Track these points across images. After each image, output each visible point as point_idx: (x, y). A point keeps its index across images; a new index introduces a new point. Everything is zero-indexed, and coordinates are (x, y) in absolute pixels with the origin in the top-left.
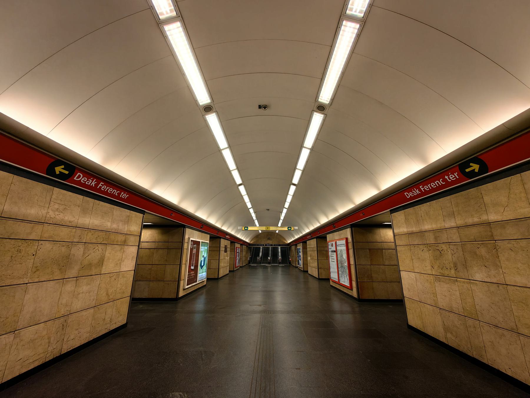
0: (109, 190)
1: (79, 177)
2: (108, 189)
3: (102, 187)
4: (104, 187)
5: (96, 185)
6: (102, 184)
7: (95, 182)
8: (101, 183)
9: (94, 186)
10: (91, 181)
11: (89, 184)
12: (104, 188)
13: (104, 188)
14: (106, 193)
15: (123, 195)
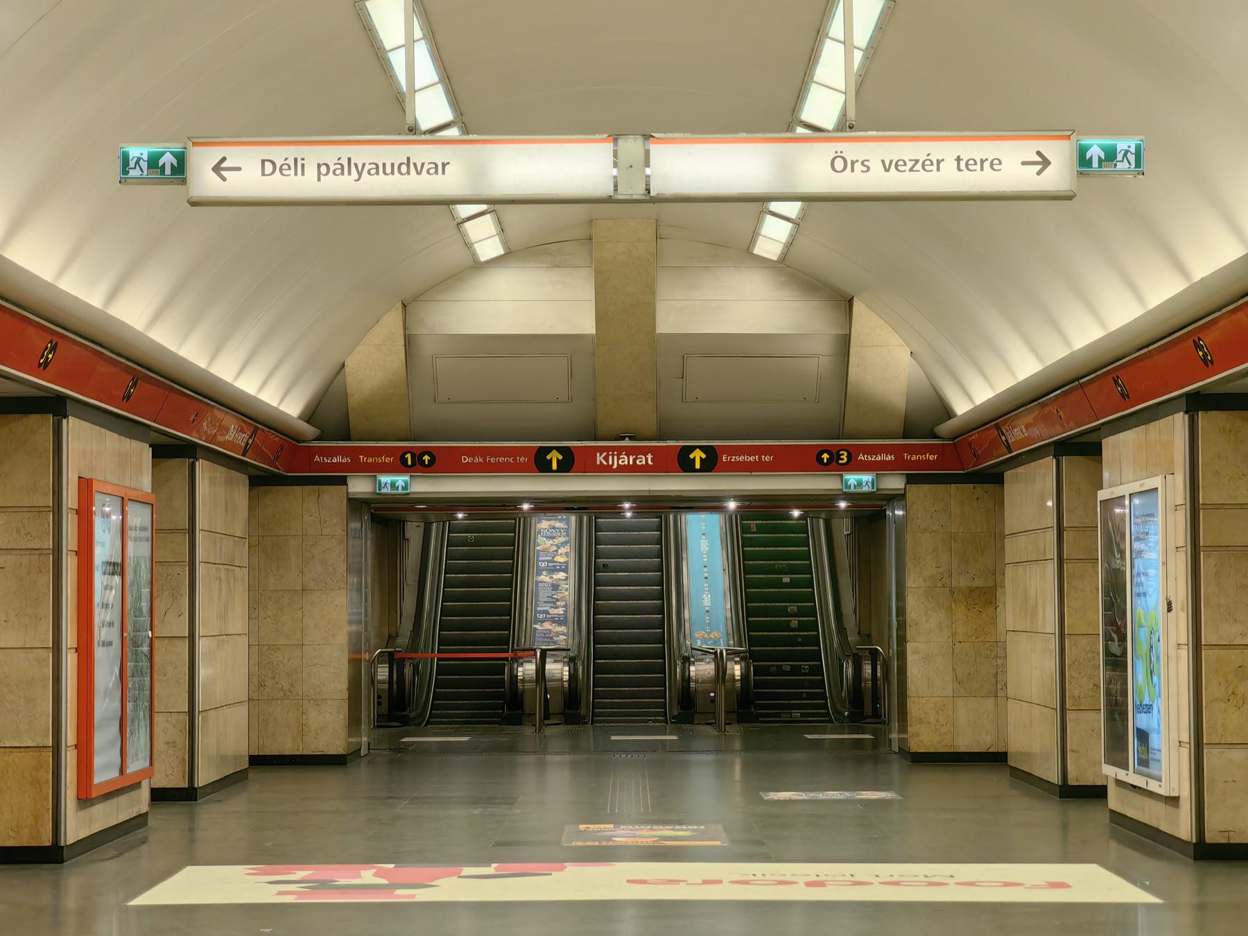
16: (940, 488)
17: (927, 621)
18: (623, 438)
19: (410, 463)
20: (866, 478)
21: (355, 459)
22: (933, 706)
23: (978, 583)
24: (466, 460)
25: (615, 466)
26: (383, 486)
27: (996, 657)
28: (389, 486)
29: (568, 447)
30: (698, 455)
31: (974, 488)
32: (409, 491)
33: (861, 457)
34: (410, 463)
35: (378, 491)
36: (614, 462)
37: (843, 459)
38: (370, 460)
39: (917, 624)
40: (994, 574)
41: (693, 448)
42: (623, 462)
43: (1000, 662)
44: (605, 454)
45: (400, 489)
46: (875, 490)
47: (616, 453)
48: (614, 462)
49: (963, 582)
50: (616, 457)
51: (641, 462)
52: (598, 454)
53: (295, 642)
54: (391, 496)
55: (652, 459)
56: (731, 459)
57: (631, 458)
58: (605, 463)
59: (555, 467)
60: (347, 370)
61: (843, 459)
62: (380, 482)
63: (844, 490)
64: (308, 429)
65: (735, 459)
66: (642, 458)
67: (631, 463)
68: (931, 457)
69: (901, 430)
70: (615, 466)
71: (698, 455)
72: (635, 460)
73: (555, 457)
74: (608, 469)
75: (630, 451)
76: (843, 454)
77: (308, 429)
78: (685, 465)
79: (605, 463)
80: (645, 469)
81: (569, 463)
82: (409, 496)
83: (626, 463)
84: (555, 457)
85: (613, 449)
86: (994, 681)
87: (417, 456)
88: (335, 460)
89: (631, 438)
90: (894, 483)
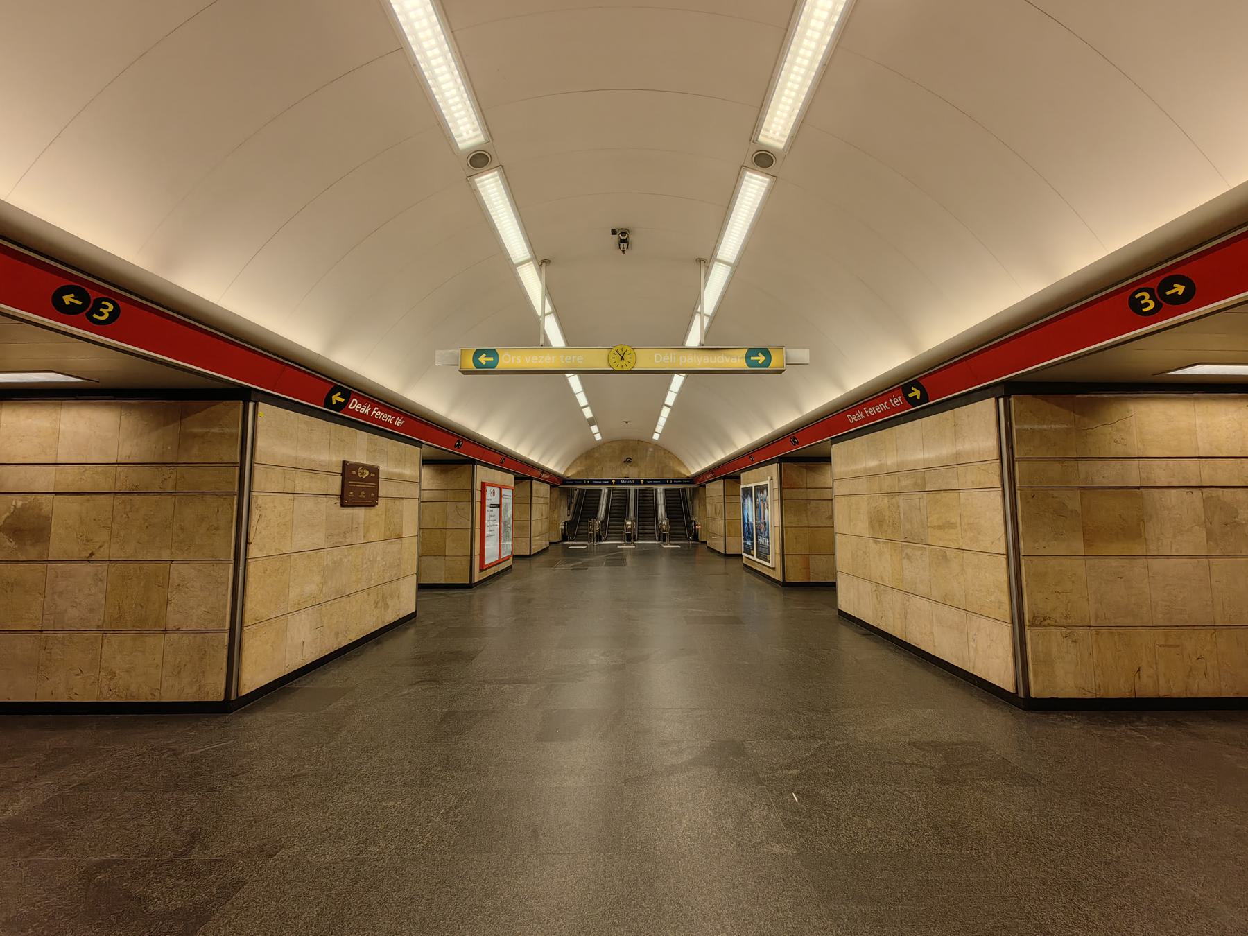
1: (355, 405)
5: (370, 412)
6: (377, 411)
12: (377, 414)
13: (377, 414)
14: (379, 421)
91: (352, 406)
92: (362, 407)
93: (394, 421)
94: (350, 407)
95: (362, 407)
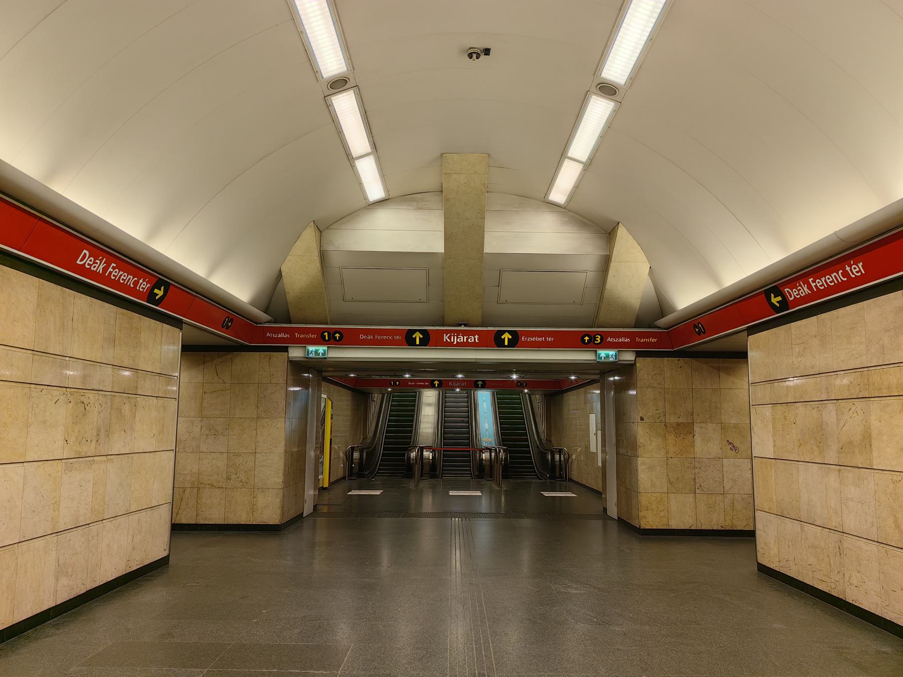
0: (122, 277)
2: (121, 275)
3: (112, 272)
4: (116, 272)
5: (105, 270)
6: (114, 268)
7: (104, 264)
8: (113, 265)
9: (101, 272)
10: (98, 262)
11: (95, 269)
12: (115, 273)
13: (115, 273)
14: (116, 284)
15: (141, 283)
16: (658, 360)
17: (650, 444)
18: (460, 325)
19: (327, 339)
20: (612, 353)
21: (292, 336)
22: (655, 498)
23: (681, 420)
24: (363, 337)
25: (455, 343)
26: (310, 352)
27: (695, 468)
28: (314, 353)
29: (426, 330)
30: (506, 336)
31: (679, 360)
32: (326, 356)
33: (609, 339)
34: (327, 339)
35: (307, 356)
36: (455, 340)
37: (597, 341)
38: (302, 336)
39: (644, 446)
40: (692, 415)
41: (504, 332)
42: (460, 340)
43: (697, 470)
44: (449, 335)
45: (321, 355)
46: (617, 360)
47: (456, 334)
48: (455, 340)
49: (673, 419)
50: (456, 337)
51: (471, 340)
52: (445, 335)
53: (251, 451)
54: (316, 360)
55: (478, 338)
56: (527, 339)
57: (465, 338)
58: (449, 341)
59: (418, 343)
60: (285, 279)
61: (597, 341)
62: (308, 350)
63: (598, 360)
64: (263, 316)
65: (530, 339)
66: (471, 338)
67: (465, 341)
68: (653, 340)
69: (633, 323)
70: (455, 343)
71: (506, 336)
72: (467, 339)
73: (418, 336)
74: (451, 344)
75: (464, 333)
76: (598, 337)
77: (263, 316)
78: (498, 343)
79: (449, 341)
80: (474, 345)
81: (427, 340)
82: (326, 360)
83: (462, 341)
84: (418, 336)
85: (454, 331)
86: (693, 483)
87: (332, 333)
88: (280, 336)
89: (466, 325)
90: (628, 356)
91: (80, 261)
92: (94, 263)
93: (136, 283)
94: (78, 262)
95: (94, 263)
